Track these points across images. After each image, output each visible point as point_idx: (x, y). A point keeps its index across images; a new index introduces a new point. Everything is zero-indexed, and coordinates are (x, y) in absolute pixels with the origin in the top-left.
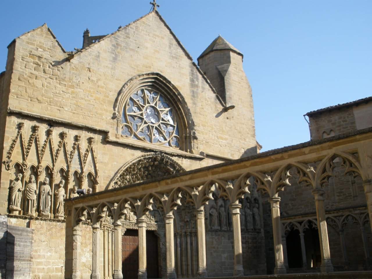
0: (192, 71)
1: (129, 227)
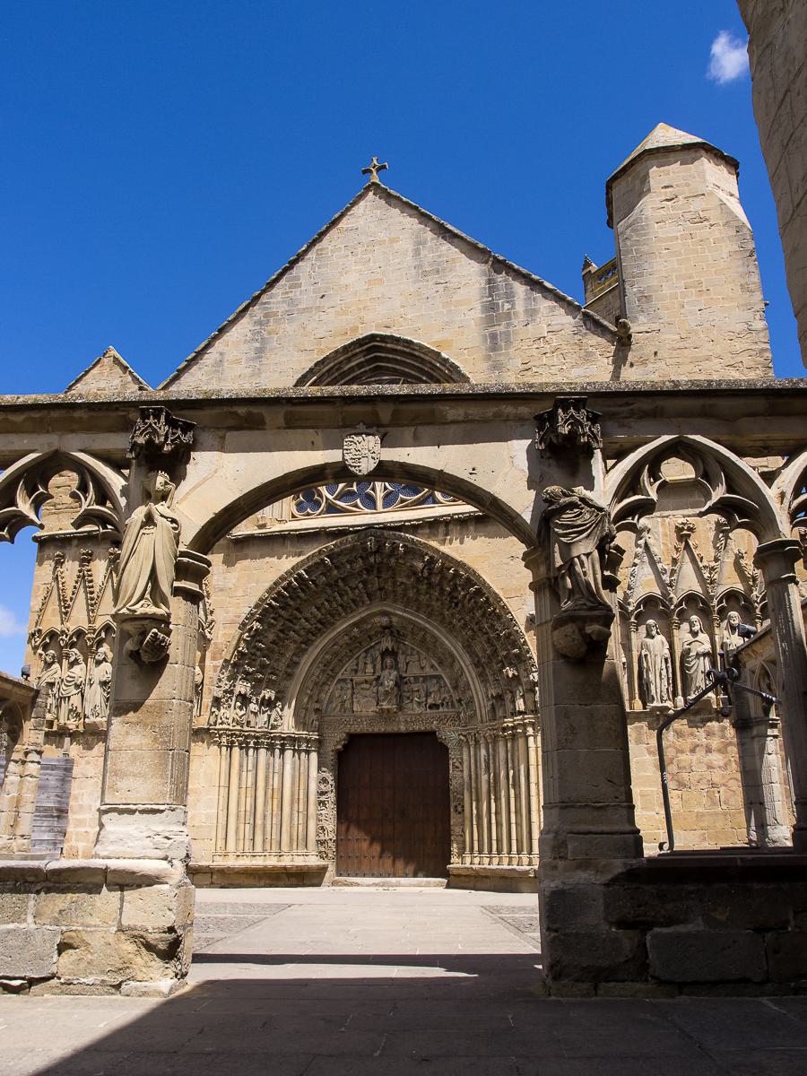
0: (489, 281)
1: (352, 731)
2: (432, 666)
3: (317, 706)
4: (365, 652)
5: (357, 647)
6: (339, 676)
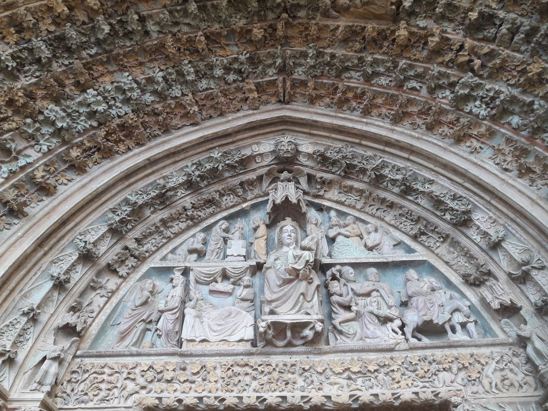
2: (399, 244)
3: (71, 319)
4: (225, 218)
5: (210, 202)
6: (155, 262)
